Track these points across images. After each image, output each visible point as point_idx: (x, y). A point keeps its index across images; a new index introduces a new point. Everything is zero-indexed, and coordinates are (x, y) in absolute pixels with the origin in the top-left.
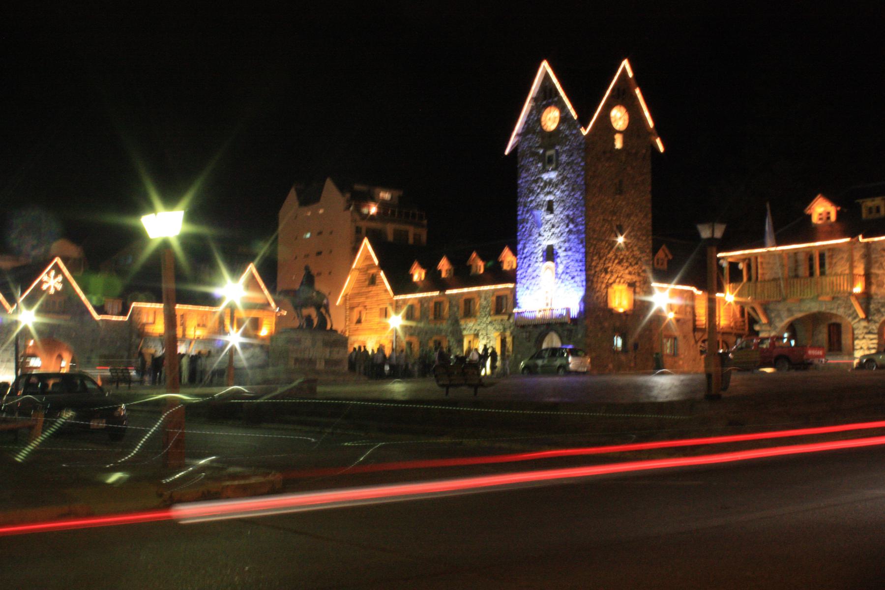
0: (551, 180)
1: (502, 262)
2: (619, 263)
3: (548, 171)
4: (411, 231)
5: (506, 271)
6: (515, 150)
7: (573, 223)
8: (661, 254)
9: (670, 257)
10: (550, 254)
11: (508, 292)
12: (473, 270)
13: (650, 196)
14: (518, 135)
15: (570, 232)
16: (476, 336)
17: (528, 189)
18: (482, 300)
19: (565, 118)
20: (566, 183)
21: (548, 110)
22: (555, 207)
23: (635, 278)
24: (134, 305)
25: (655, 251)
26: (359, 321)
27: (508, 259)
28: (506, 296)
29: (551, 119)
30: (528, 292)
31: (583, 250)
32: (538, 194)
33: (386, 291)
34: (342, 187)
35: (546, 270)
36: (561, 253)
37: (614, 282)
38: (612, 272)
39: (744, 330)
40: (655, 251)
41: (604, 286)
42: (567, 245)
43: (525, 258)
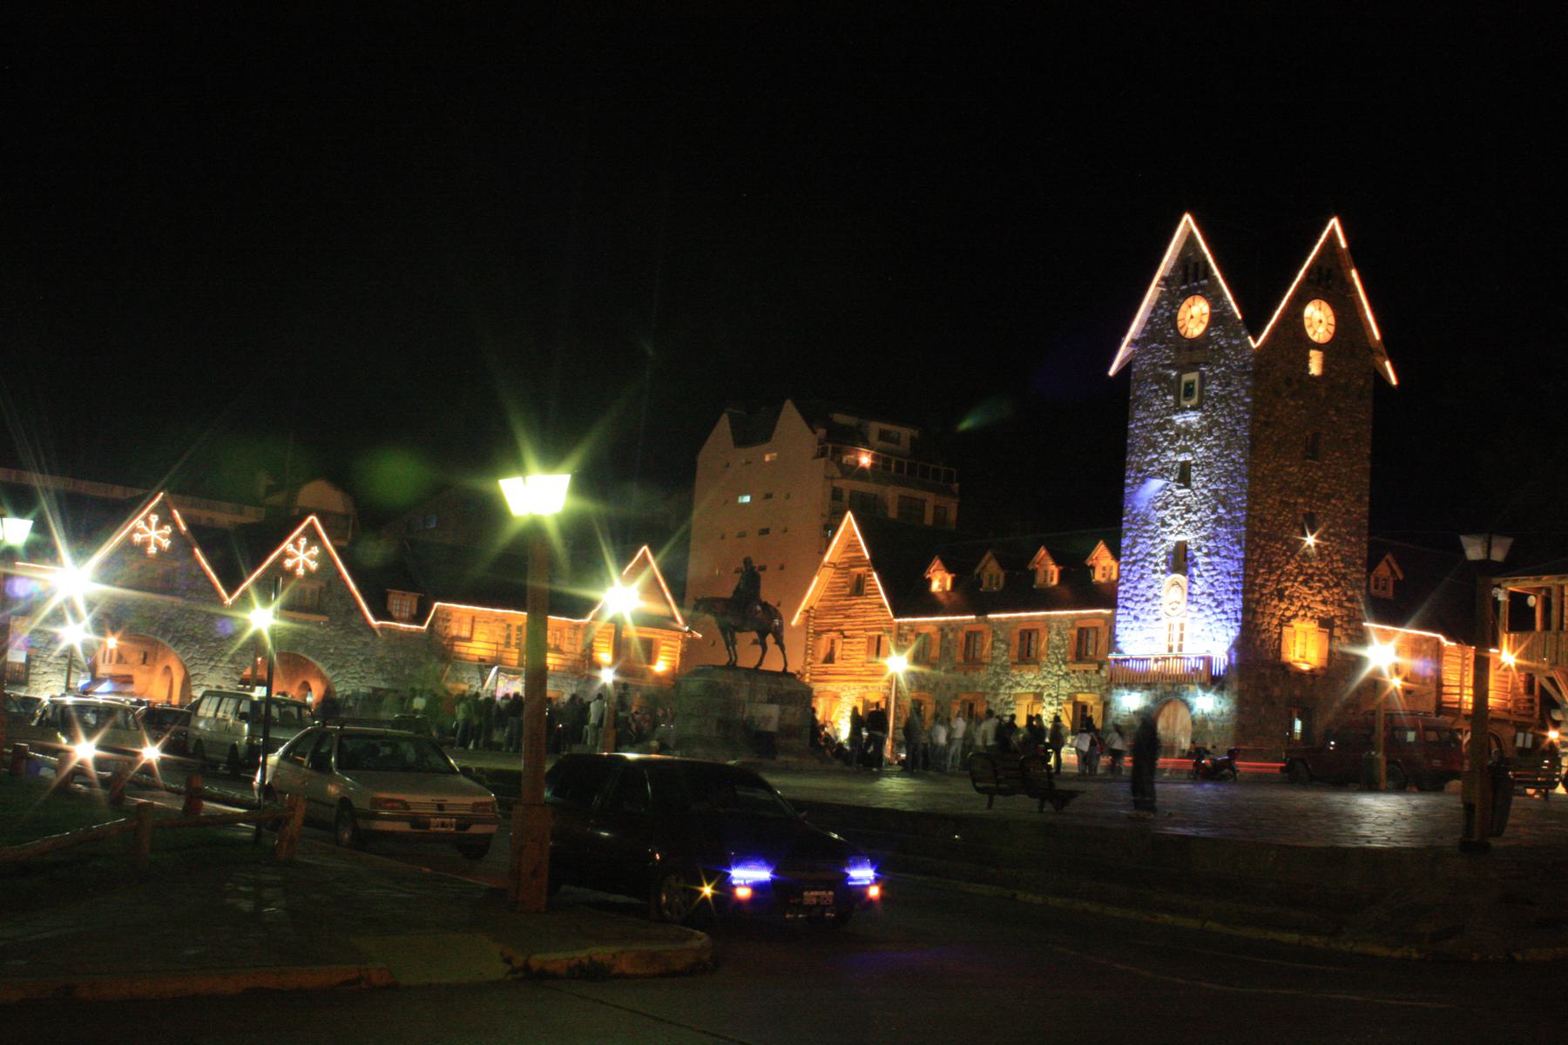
0: (1189, 425)
1: (1093, 567)
3: (1183, 410)
4: (931, 500)
5: (1098, 585)
6: (1126, 369)
8: (1383, 570)
9: (1401, 577)
10: (1180, 560)
11: (1099, 623)
12: (1039, 579)
13: (1368, 465)
14: (1134, 342)
15: (1218, 521)
16: (1038, 697)
19: (1218, 317)
21: (1190, 300)
23: (1332, 611)
24: (437, 604)
25: (1371, 564)
26: (830, 659)
27: (1102, 563)
28: (1096, 629)
29: (1195, 316)
30: (1136, 624)
31: (1241, 555)
33: (882, 606)
34: (811, 418)
35: (1171, 588)
37: (1295, 616)
38: (1291, 598)
39: (1531, 716)
40: (1371, 564)
41: (1275, 622)
42: (1211, 544)
43: (1134, 563)
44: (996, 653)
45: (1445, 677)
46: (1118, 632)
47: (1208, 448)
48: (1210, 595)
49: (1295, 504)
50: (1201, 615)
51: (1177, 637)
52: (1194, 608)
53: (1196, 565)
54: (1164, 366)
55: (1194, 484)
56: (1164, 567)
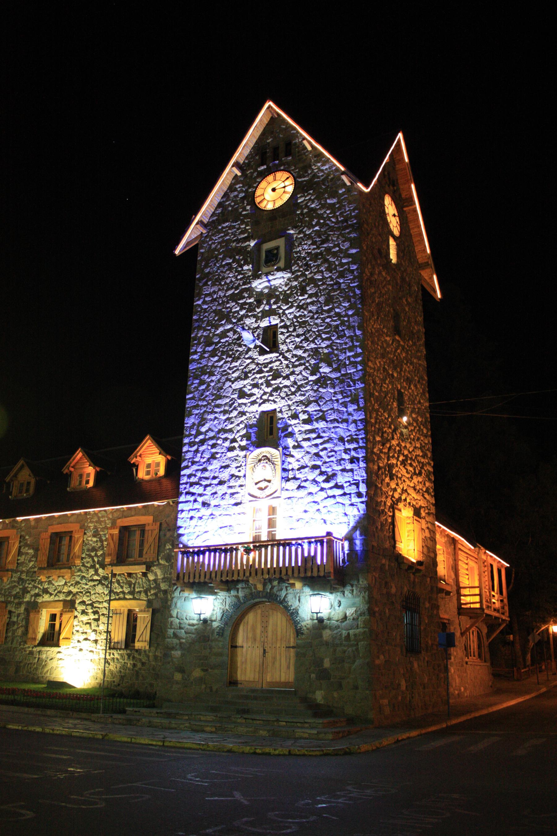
1: (137, 467)
2: (403, 463)
6: (192, 252)
7: (329, 365)
10: (268, 432)
12: (74, 483)
14: (200, 222)
16: (70, 605)
18: (89, 533)
20: (311, 290)
21: (270, 178)
22: (281, 338)
27: (150, 459)
28: (142, 528)
29: (275, 191)
30: (204, 512)
36: (297, 427)
43: (202, 442)
44: (22, 559)
45: (461, 579)
46: (180, 523)
47: (299, 307)
48: (315, 467)
49: (392, 375)
50: (302, 492)
52: (292, 485)
53: (291, 435)
54: (238, 241)
55: (283, 348)
56: (244, 443)
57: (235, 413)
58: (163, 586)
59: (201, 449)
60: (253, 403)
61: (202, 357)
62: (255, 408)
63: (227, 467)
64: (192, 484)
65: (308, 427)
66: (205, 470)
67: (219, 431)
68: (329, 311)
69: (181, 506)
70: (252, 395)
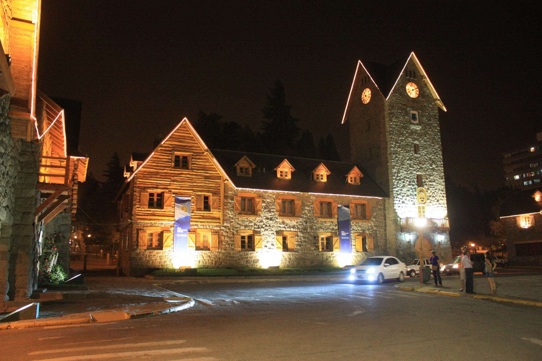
0: (416, 130)
17: (399, 131)
31: (444, 184)
32: (407, 137)
43: (400, 180)
47: (425, 141)
51: (422, 212)
57: (409, 172)
58: (375, 228)
59: (400, 182)
60: (414, 170)
61: (395, 147)
62: (415, 172)
63: (409, 191)
64: (398, 194)
65: (431, 183)
66: (401, 190)
67: (405, 177)
68: (434, 146)
69: (395, 202)
70: (414, 167)
